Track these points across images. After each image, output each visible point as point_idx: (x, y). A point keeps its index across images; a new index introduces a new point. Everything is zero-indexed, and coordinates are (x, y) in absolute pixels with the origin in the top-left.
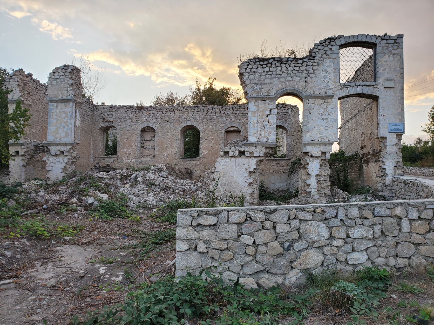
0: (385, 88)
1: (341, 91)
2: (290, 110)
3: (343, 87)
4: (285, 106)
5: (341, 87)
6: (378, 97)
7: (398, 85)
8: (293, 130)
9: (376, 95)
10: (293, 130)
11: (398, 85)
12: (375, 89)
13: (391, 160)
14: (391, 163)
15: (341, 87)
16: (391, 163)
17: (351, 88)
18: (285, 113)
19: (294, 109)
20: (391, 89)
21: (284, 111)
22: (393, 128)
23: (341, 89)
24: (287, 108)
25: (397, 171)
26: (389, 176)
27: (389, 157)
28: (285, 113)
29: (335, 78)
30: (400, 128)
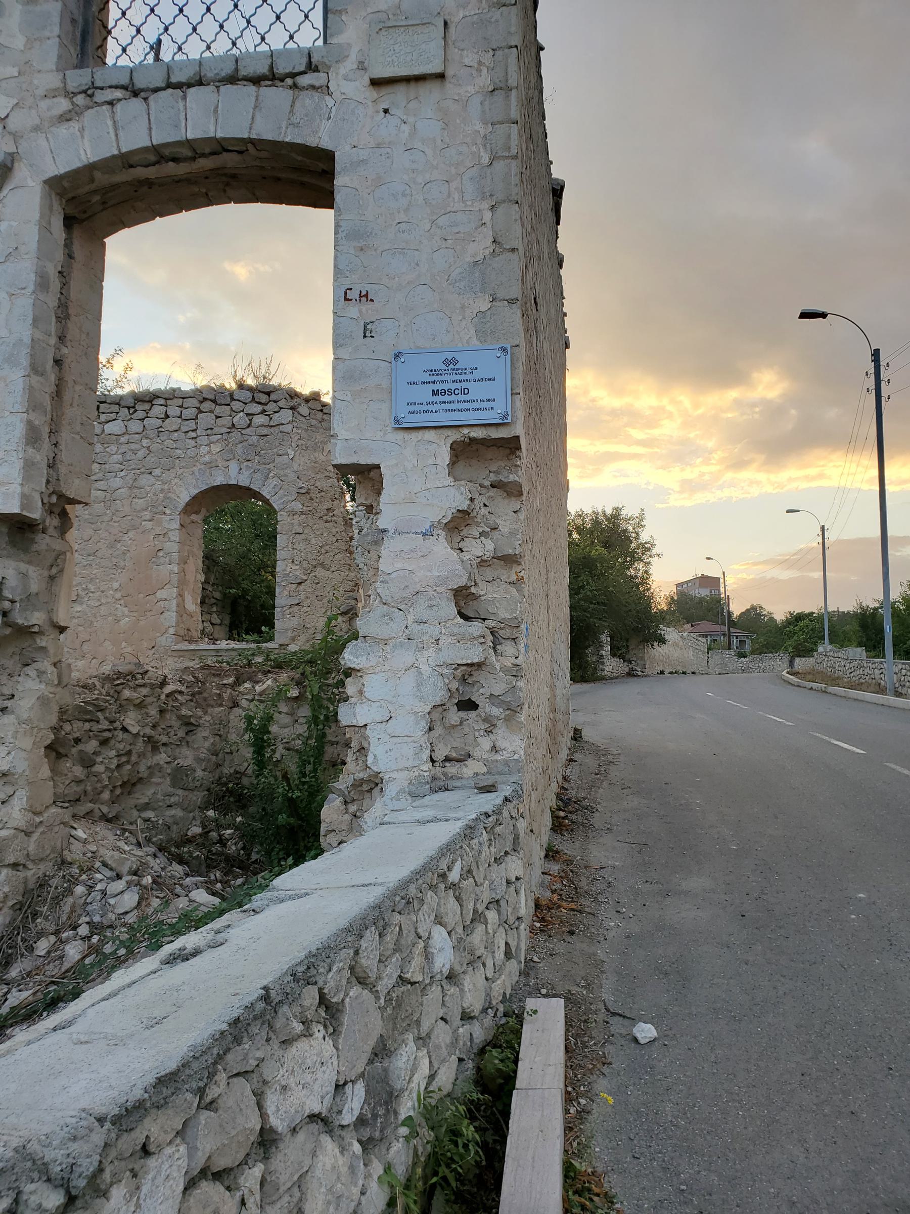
0: (376, 83)
1: (63, 131)
2: (286, 415)
3: (80, 100)
4: (263, 398)
5: (63, 105)
6: (329, 156)
7: (470, 59)
8: (298, 506)
9: (312, 142)
10: (298, 506)
11: (470, 59)
12: (307, 100)
13: (406, 657)
14: (408, 681)
15: (63, 105)
16: (410, 679)
17: (136, 104)
18: (265, 431)
19: (304, 410)
20: (424, 89)
21: (260, 420)
22: (424, 394)
23: (65, 118)
24: (271, 407)
25: (486, 743)
26: (391, 789)
27: (394, 629)
28: (265, 431)
29: (30, 43)
30: (477, 391)
